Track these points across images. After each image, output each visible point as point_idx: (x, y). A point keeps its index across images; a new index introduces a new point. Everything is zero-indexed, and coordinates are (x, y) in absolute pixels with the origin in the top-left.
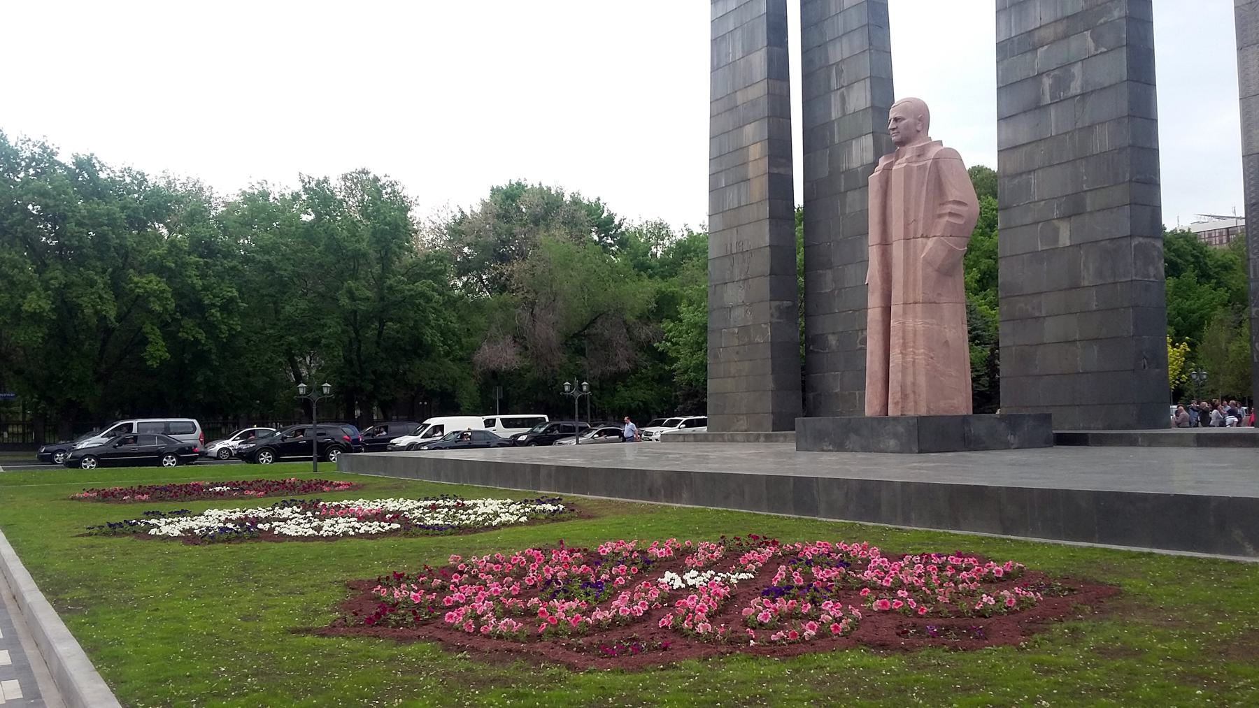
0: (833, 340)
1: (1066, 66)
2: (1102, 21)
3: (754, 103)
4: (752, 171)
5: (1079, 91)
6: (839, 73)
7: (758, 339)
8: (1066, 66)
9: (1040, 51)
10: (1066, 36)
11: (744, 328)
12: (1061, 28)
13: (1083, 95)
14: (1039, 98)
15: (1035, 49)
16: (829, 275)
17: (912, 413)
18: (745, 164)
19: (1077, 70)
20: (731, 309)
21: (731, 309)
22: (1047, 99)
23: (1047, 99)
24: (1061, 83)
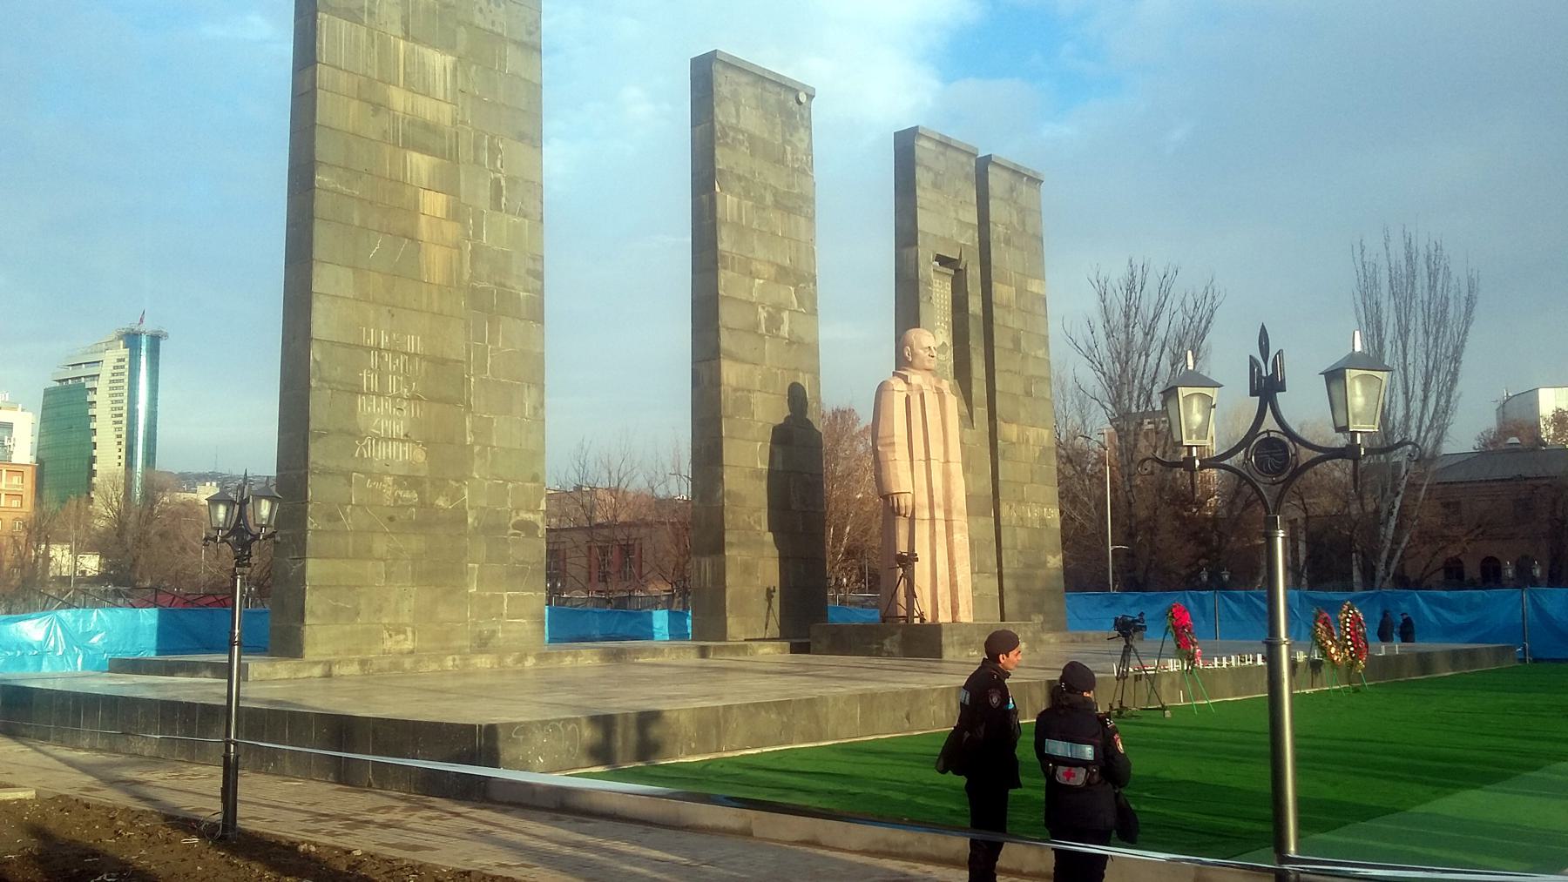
1: (779, 308)
3: (429, 128)
4: (424, 229)
6: (494, 151)
7: (441, 502)
8: (779, 308)
10: (776, 281)
11: (410, 480)
12: (773, 271)
13: (791, 343)
14: (758, 325)
15: (753, 275)
18: (414, 211)
19: (785, 315)
20: (378, 439)
21: (378, 439)
22: (763, 329)
23: (763, 329)
24: (774, 322)
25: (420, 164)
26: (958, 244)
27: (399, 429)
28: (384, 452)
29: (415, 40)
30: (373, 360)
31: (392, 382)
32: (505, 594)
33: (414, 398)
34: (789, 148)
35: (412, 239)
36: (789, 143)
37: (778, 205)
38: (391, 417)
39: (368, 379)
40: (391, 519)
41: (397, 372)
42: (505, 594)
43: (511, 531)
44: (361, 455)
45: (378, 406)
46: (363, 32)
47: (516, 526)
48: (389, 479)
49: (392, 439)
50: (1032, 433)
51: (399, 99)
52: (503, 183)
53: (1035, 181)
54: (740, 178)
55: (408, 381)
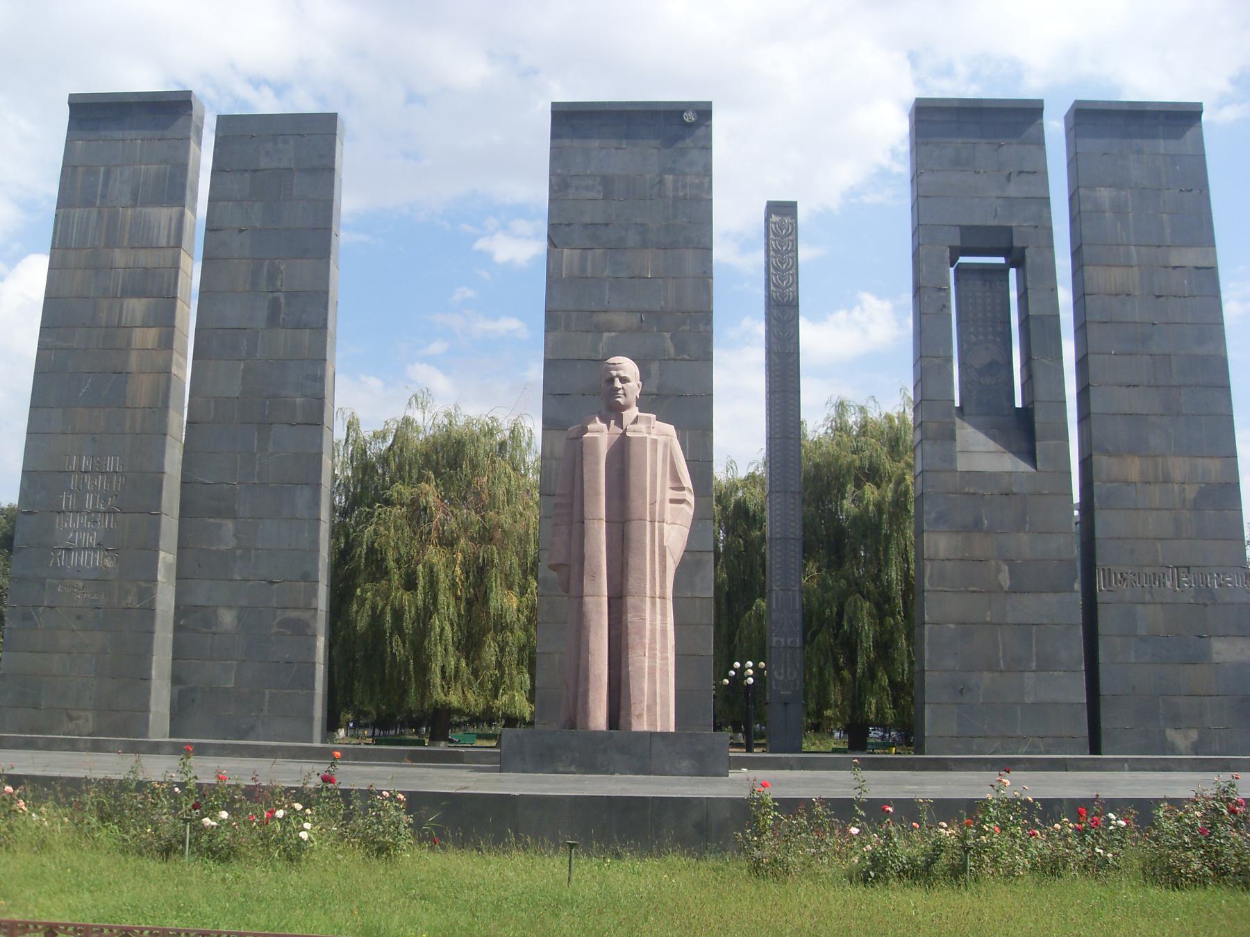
0: (227, 618)
2: (687, 328)
4: (134, 361)
5: (654, 390)
9: (606, 335)
12: (634, 319)
15: (599, 329)
16: (229, 525)
17: (659, 730)
20: (68, 550)
25: (136, 307)
26: (1008, 231)
27: (92, 540)
28: (76, 559)
29: (144, 204)
30: (74, 481)
31: (89, 499)
32: (267, 692)
33: (110, 512)
34: (669, 178)
35: (122, 373)
36: (671, 171)
37: (644, 245)
38: (86, 530)
39: (66, 500)
40: (79, 618)
41: (95, 491)
42: (267, 692)
43: (275, 629)
44: (55, 563)
45: (75, 521)
46: (94, 212)
47: (285, 623)
48: (81, 584)
49: (85, 549)
50: (1179, 467)
51: (120, 257)
52: (282, 300)
53: (1183, 118)
54: (586, 225)
55: (105, 499)
